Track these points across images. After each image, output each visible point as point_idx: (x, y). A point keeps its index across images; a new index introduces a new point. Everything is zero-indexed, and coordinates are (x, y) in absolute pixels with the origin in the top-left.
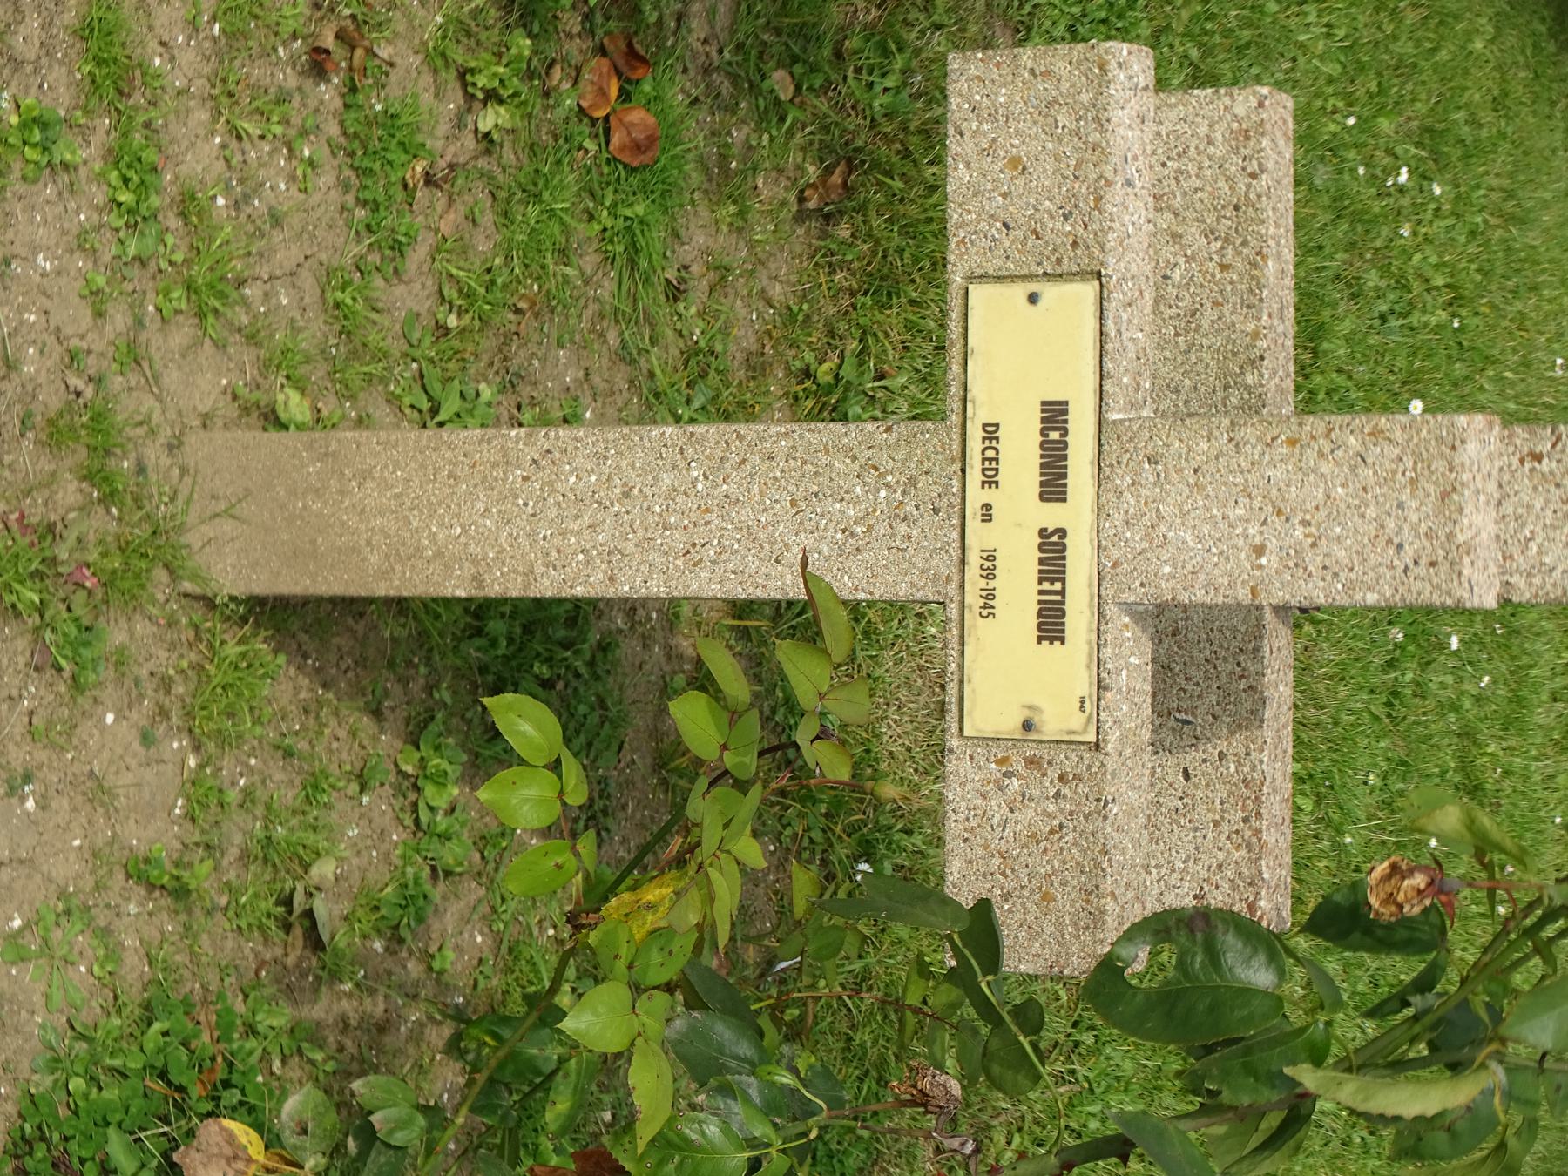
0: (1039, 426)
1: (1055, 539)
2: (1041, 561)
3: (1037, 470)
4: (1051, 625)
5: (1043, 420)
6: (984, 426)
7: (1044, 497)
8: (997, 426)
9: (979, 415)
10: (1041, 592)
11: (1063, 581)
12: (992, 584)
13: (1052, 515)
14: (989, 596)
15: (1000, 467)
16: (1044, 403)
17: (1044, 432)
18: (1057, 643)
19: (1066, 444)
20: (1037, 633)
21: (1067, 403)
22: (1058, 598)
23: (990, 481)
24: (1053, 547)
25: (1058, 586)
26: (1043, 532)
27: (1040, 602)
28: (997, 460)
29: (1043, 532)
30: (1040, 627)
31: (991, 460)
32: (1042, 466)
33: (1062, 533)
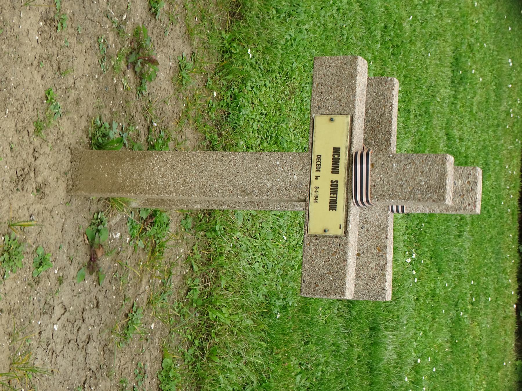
0: (332, 154)
1: (335, 183)
2: (331, 189)
4: (333, 205)
5: (333, 152)
7: (332, 172)
10: (330, 197)
11: (337, 194)
13: (335, 177)
14: (316, 197)
16: (334, 148)
17: (333, 156)
20: (329, 208)
24: (334, 186)
25: (335, 196)
30: (330, 206)
33: (337, 182)
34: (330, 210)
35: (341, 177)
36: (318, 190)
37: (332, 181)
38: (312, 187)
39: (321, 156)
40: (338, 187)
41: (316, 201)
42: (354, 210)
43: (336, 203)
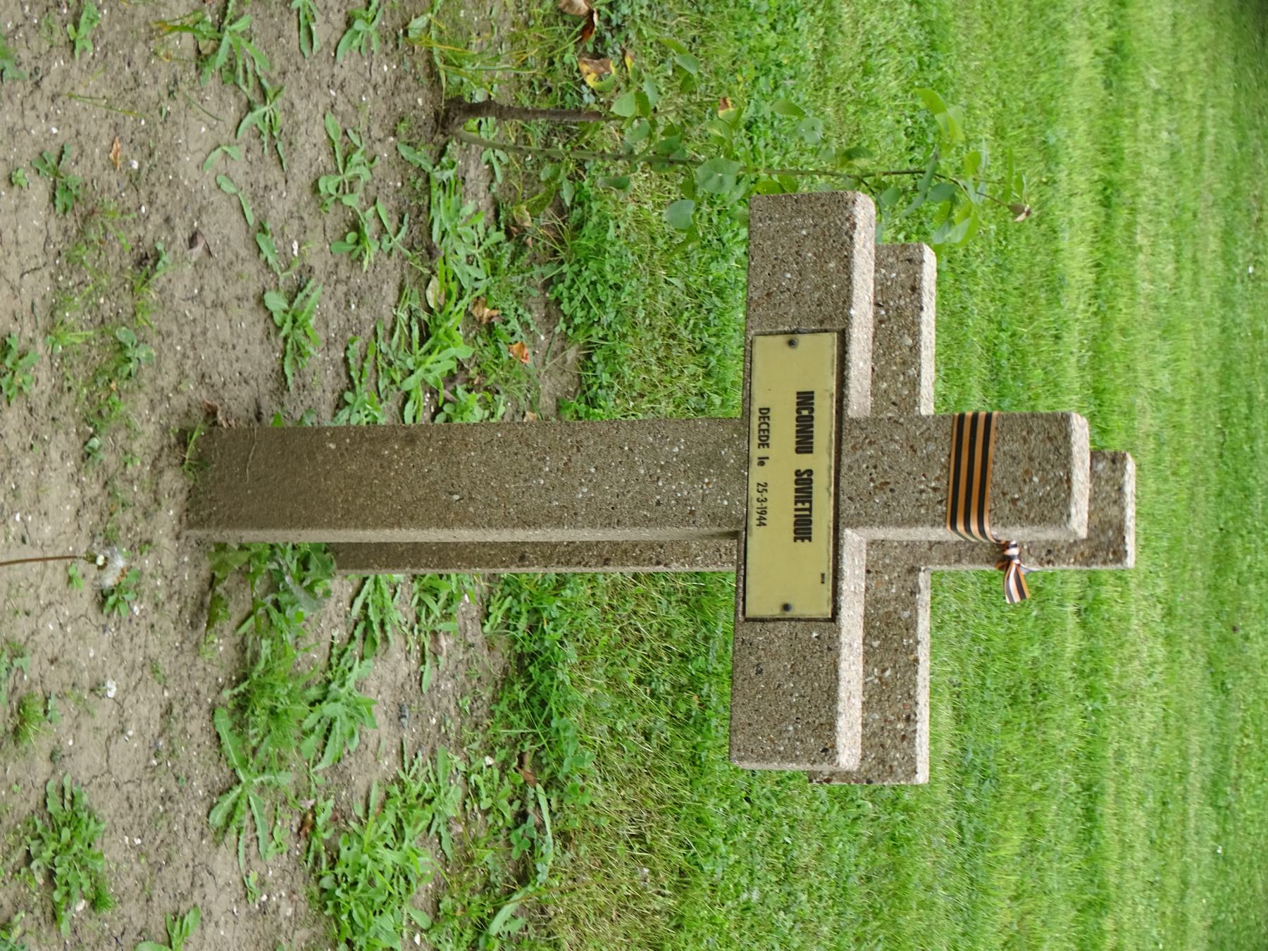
0: (795, 407)
2: (797, 490)
3: (794, 434)
4: (803, 529)
5: (798, 404)
6: (760, 410)
7: (798, 451)
10: (796, 510)
11: (810, 502)
12: (764, 504)
13: (804, 462)
15: (771, 435)
16: (798, 393)
17: (798, 411)
18: (807, 541)
19: (812, 418)
20: (793, 535)
23: (764, 443)
25: (807, 505)
26: (798, 473)
30: (796, 532)
32: (798, 432)
33: (810, 472)
34: (795, 540)
35: (820, 462)
37: (798, 473)
39: (768, 409)
40: (814, 485)
43: (810, 522)
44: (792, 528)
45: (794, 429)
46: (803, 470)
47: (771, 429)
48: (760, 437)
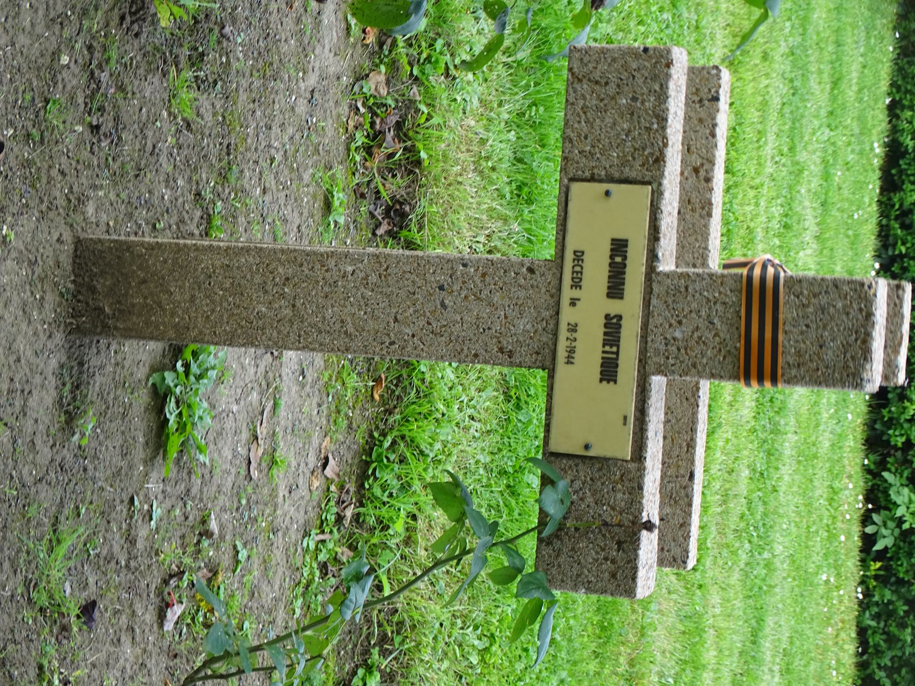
0: (608, 253)
1: (615, 321)
2: (605, 334)
3: (606, 280)
4: (609, 371)
5: (612, 250)
6: (575, 252)
7: (610, 295)
8: (583, 253)
9: (572, 245)
10: (604, 352)
13: (614, 307)
15: (584, 277)
16: (613, 240)
17: (612, 257)
18: (612, 383)
20: (599, 376)
21: (627, 241)
22: (614, 356)
25: (614, 349)
27: (603, 358)
28: (581, 273)
29: (607, 317)
30: (601, 373)
31: (577, 272)
33: (620, 317)
34: (601, 380)
36: (575, 335)
38: (563, 327)
41: (569, 361)
42: (658, 383)
43: (617, 366)
44: (599, 369)
45: (606, 274)
46: (612, 315)
47: (584, 271)
48: (573, 278)
